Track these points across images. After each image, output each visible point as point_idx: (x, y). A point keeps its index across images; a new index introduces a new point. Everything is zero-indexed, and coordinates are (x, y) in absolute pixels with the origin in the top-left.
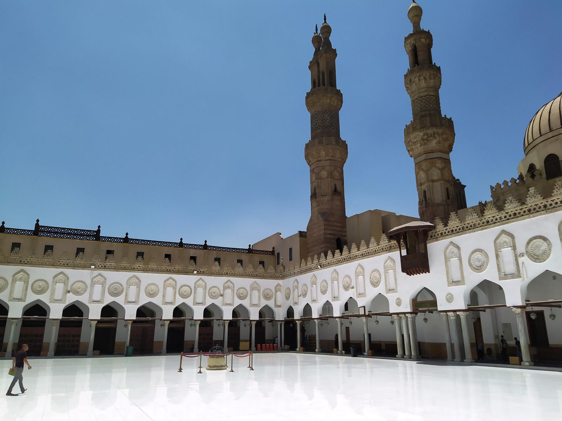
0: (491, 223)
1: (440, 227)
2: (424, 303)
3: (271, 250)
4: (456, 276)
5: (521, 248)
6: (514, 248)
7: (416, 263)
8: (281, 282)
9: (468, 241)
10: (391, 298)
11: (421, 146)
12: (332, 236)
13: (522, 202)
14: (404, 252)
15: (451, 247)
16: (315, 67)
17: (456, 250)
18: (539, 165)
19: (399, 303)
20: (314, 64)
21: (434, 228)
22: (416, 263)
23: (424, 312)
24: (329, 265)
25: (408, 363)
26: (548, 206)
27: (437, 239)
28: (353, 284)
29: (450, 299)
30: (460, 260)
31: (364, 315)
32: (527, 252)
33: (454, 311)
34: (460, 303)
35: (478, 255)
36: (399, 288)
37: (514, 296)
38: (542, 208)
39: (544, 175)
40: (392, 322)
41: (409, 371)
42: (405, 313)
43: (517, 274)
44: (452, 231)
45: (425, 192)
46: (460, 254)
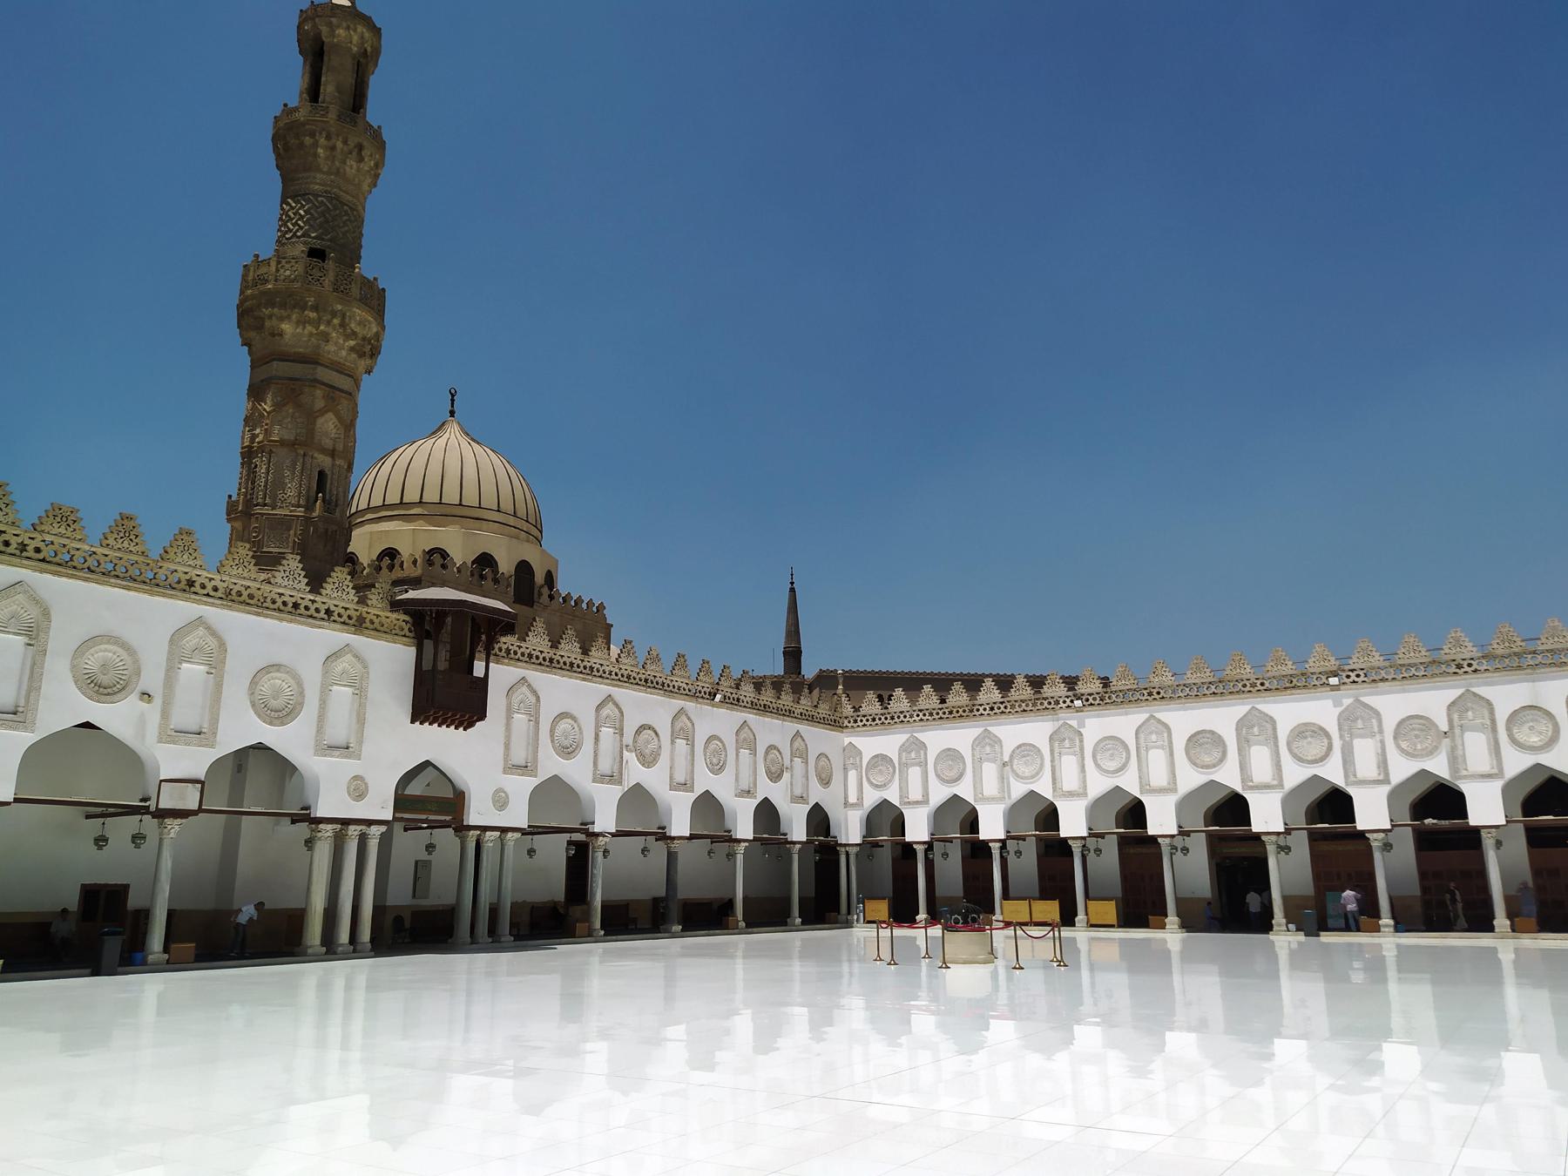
0: (234, 597)
2: (430, 802)
5: (628, 738)
7: (448, 696)
11: (352, 349)
13: (316, 582)
17: (533, 700)
19: (358, 789)
22: (448, 696)
23: (433, 826)
25: (340, 969)
26: (197, 584)
28: (152, 678)
30: (537, 722)
35: (564, 725)
36: (367, 749)
38: (183, 585)
40: (310, 843)
41: (360, 996)
42: (370, 823)
44: (530, 656)
46: (537, 712)
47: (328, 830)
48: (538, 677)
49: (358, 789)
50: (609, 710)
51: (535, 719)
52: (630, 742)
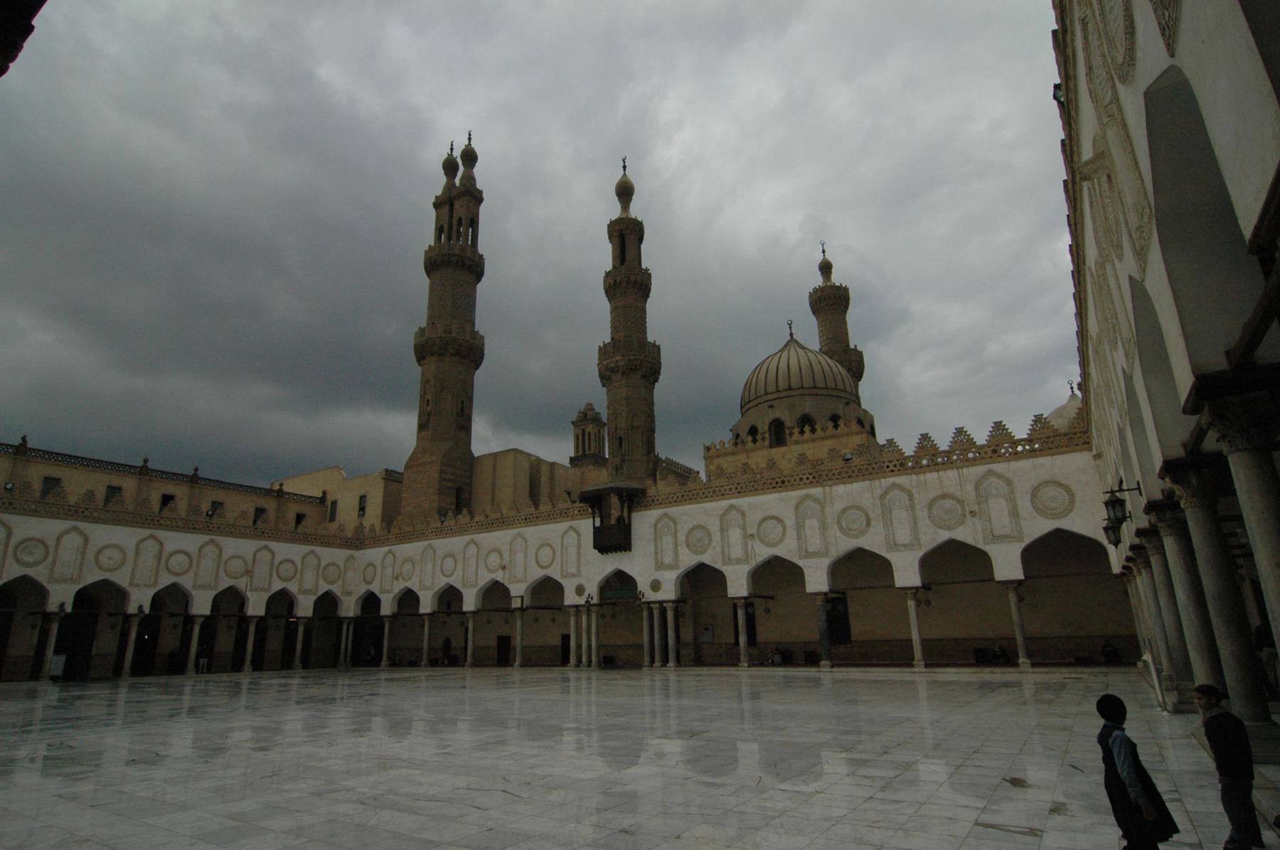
1: (651, 492)
3: (320, 495)
4: (668, 560)
6: (744, 528)
7: (613, 539)
8: (357, 553)
9: (689, 514)
10: (569, 586)
12: (450, 484)
14: (598, 524)
15: (666, 520)
16: (446, 209)
17: (671, 524)
18: (763, 427)
19: (580, 590)
20: (444, 203)
21: (644, 492)
22: (613, 539)
24: (461, 531)
27: (646, 507)
29: (656, 586)
31: (522, 609)
32: (758, 533)
33: (661, 603)
34: (669, 592)
37: (738, 586)
39: (767, 442)
43: (745, 560)
45: (621, 439)
47: (572, 610)
48: (675, 510)
49: (580, 590)
50: (734, 515)
51: (675, 534)
52: (755, 531)
